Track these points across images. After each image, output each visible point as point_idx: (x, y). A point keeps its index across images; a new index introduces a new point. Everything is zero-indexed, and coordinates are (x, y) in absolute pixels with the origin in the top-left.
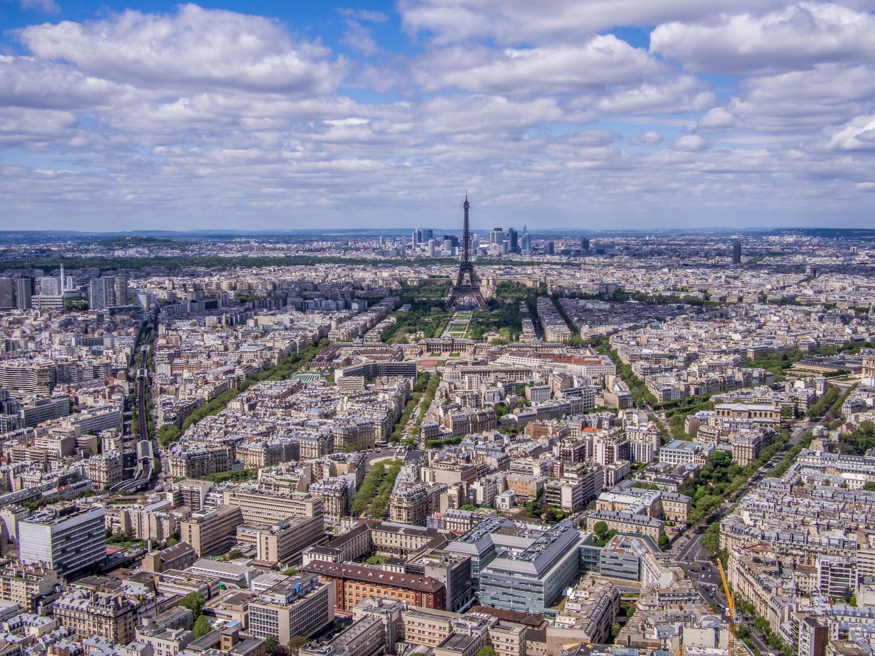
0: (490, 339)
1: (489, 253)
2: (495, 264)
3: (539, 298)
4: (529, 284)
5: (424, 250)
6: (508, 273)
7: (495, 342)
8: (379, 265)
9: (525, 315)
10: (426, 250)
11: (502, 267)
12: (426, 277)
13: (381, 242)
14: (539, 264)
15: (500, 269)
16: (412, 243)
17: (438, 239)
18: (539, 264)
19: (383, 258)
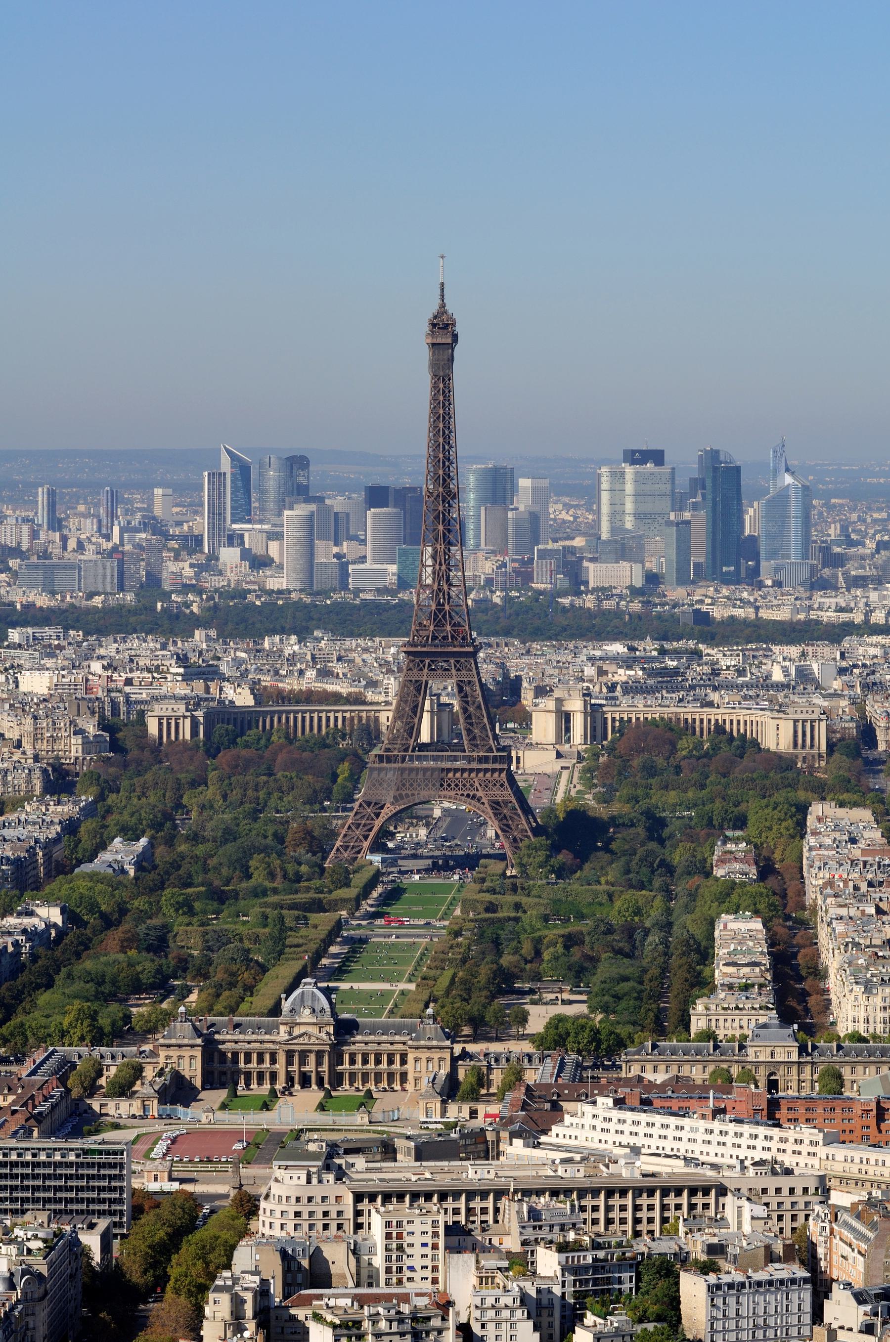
0: (538, 1018)
1: (596, 574)
2: (615, 637)
3: (818, 810)
4: (776, 735)
5: (260, 562)
6: (666, 680)
7: (557, 1037)
8: (15, 635)
9: (729, 897)
10: (277, 554)
11: (649, 647)
12: (243, 698)
13: (42, 517)
14: (835, 634)
15: (628, 663)
16: (202, 524)
17: (337, 503)
18: (835, 634)
19: (43, 601)
